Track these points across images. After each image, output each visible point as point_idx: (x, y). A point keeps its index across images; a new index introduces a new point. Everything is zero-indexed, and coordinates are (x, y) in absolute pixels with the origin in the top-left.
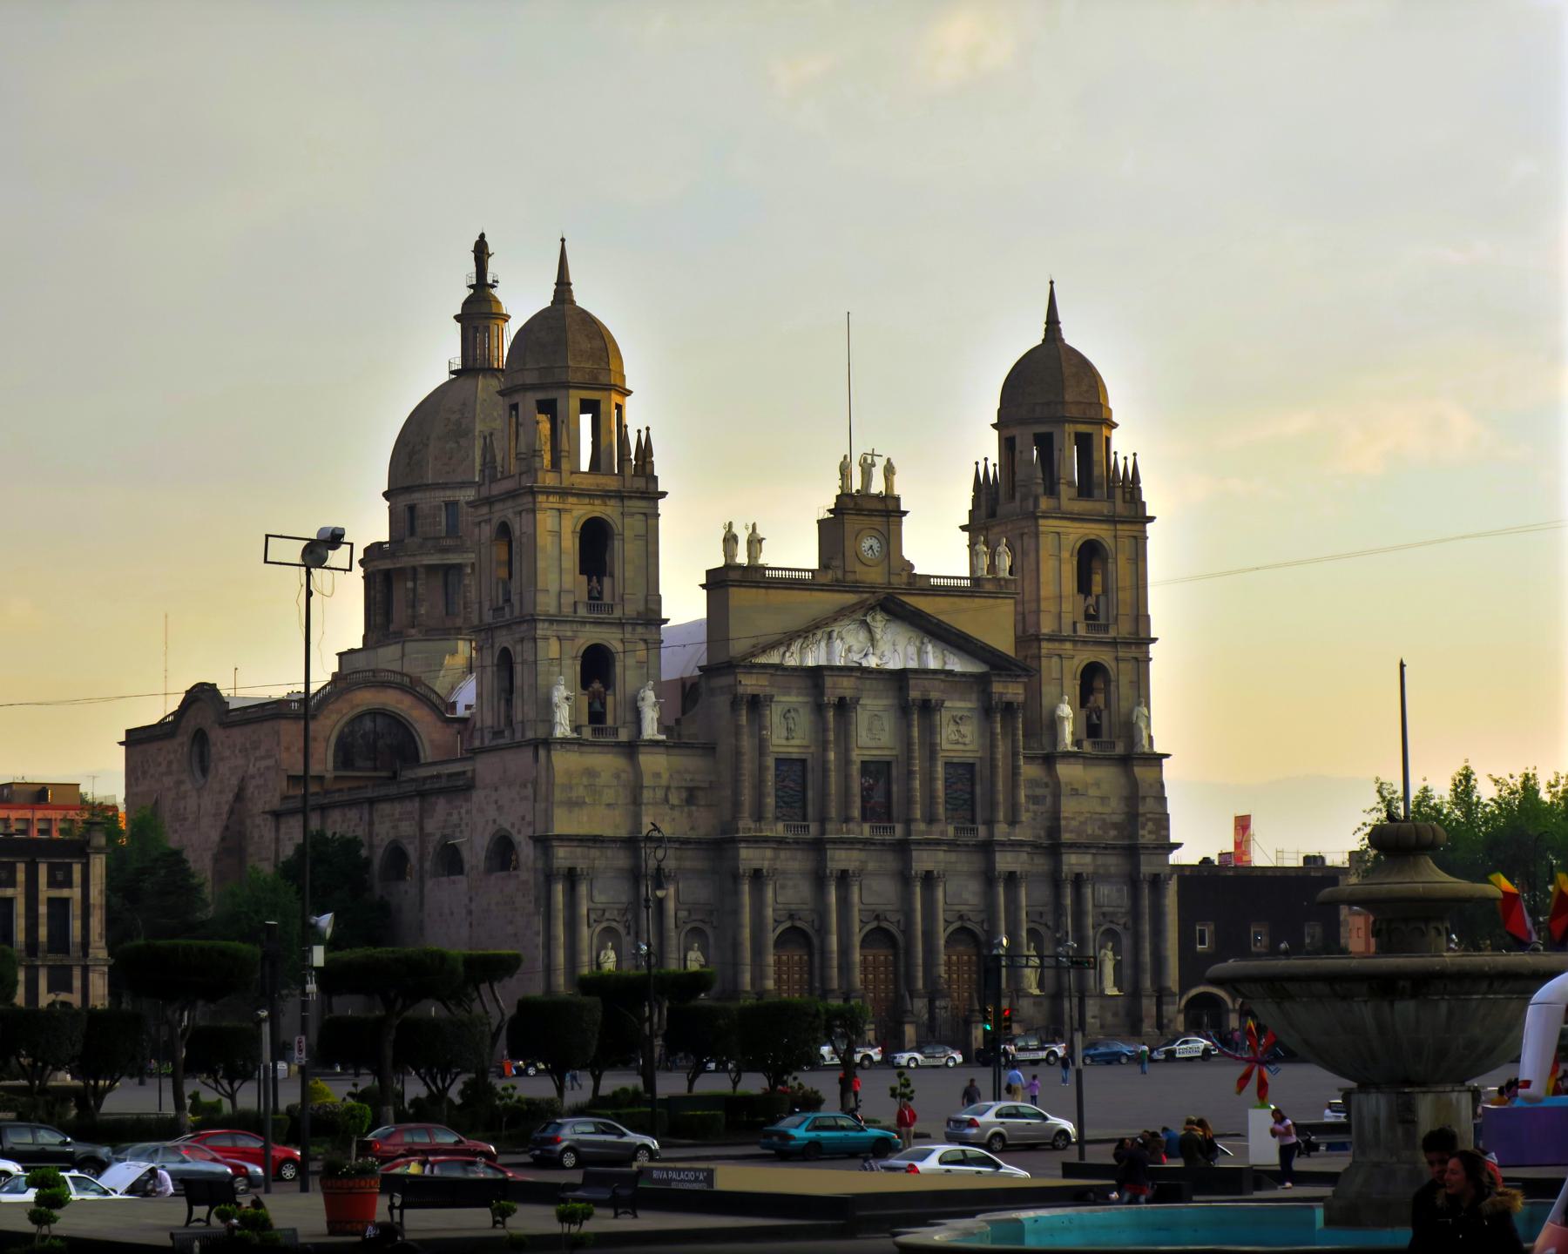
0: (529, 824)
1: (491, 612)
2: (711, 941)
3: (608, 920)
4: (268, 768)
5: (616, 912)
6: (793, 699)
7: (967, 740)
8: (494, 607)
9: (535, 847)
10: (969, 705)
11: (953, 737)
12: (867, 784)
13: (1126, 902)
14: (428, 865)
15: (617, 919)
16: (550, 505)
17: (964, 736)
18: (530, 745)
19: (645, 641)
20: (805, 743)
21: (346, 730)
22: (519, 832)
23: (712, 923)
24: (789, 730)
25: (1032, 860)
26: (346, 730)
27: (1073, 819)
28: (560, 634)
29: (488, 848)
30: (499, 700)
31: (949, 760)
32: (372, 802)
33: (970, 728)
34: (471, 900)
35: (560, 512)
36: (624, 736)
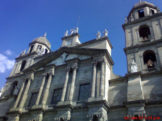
7: (87, 77)
10: (89, 67)
11: (83, 77)
12: (55, 96)
17: (87, 76)
24: (37, 85)
25: (119, 114)
27: (133, 94)
31: (81, 83)
33: (89, 73)
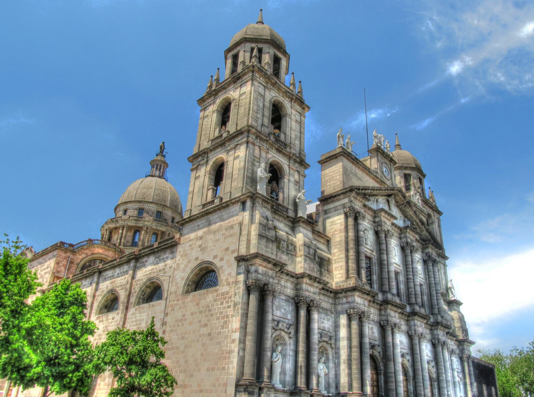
0: (233, 252)
1: (210, 142)
2: (331, 357)
3: (280, 329)
4: (46, 273)
5: (285, 325)
6: (366, 224)
8: (212, 138)
9: (238, 266)
13: (460, 367)
14: (133, 299)
15: (286, 330)
16: (261, 82)
18: (238, 202)
19: (298, 172)
20: (371, 249)
21: (87, 264)
22: (222, 259)
23: (331, 344)
26: (87, 264)
28: (261, 145)
29: (188, 279)
30: (208, 190)
32: (100, 272)
34: (166, 315)
35: (265, 88)
36: (291, 214)
